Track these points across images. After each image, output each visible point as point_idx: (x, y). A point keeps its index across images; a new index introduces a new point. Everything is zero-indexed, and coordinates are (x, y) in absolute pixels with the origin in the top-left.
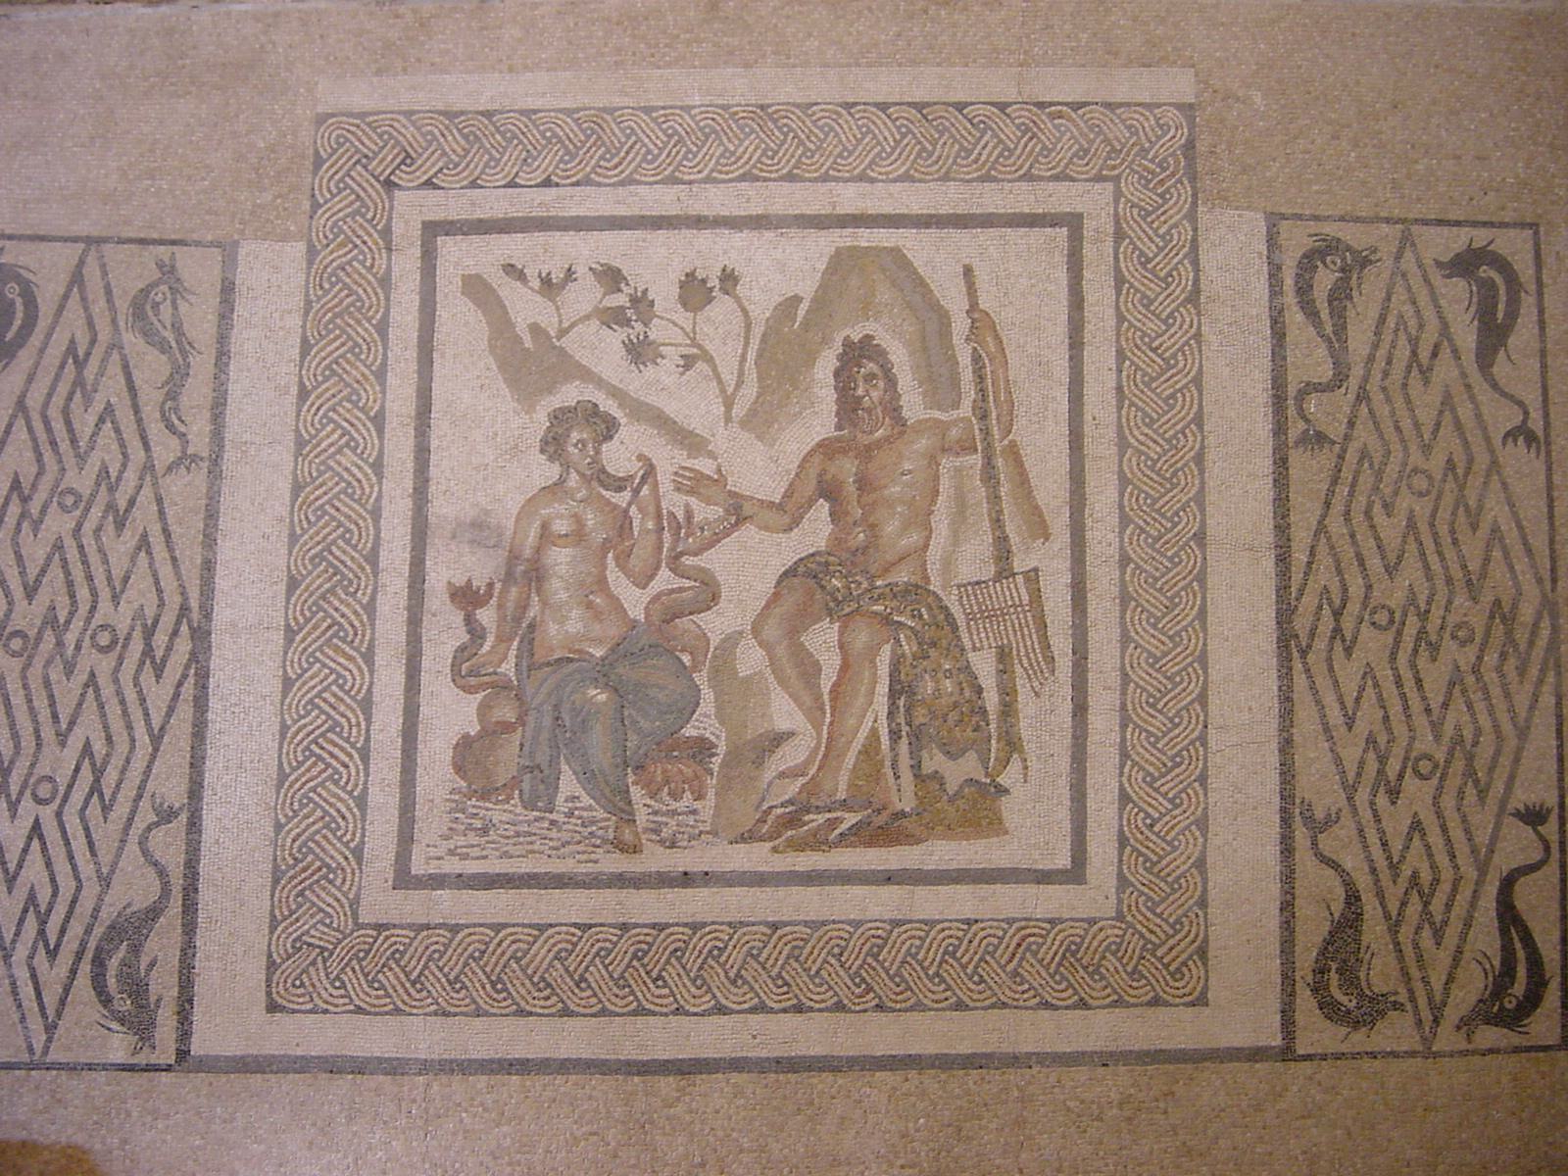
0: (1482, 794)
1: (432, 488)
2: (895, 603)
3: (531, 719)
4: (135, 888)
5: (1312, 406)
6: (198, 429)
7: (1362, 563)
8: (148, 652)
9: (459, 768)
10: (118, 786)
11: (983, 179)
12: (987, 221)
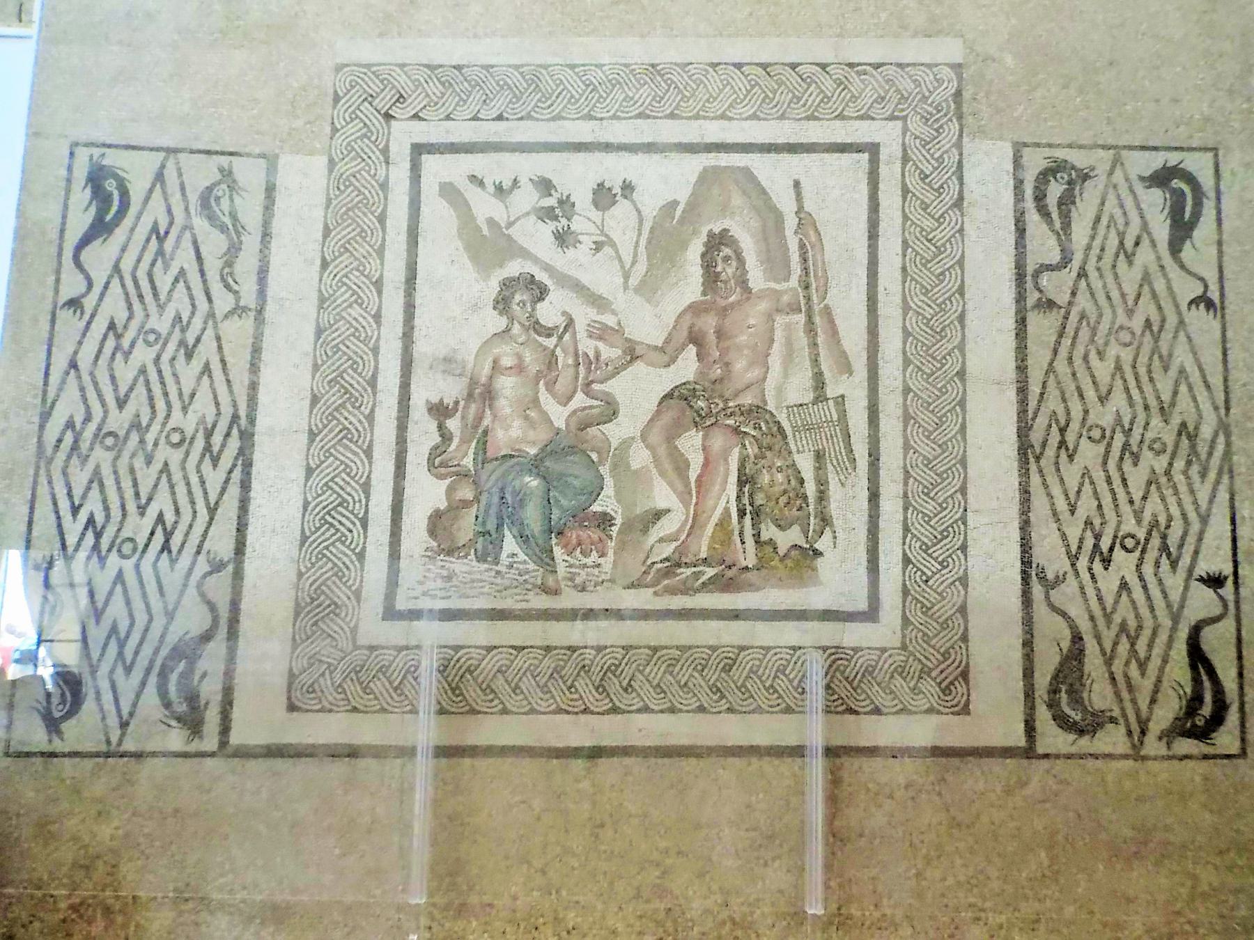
0: (1174, 564)
1: (416, 333)
2: (742, 418)
3: (484, 499)
4: (191, 620)
5: (1044, 280)
7: (1081, 396)
8: (208, 448)
9: (432, 532)
11: (808, 118)
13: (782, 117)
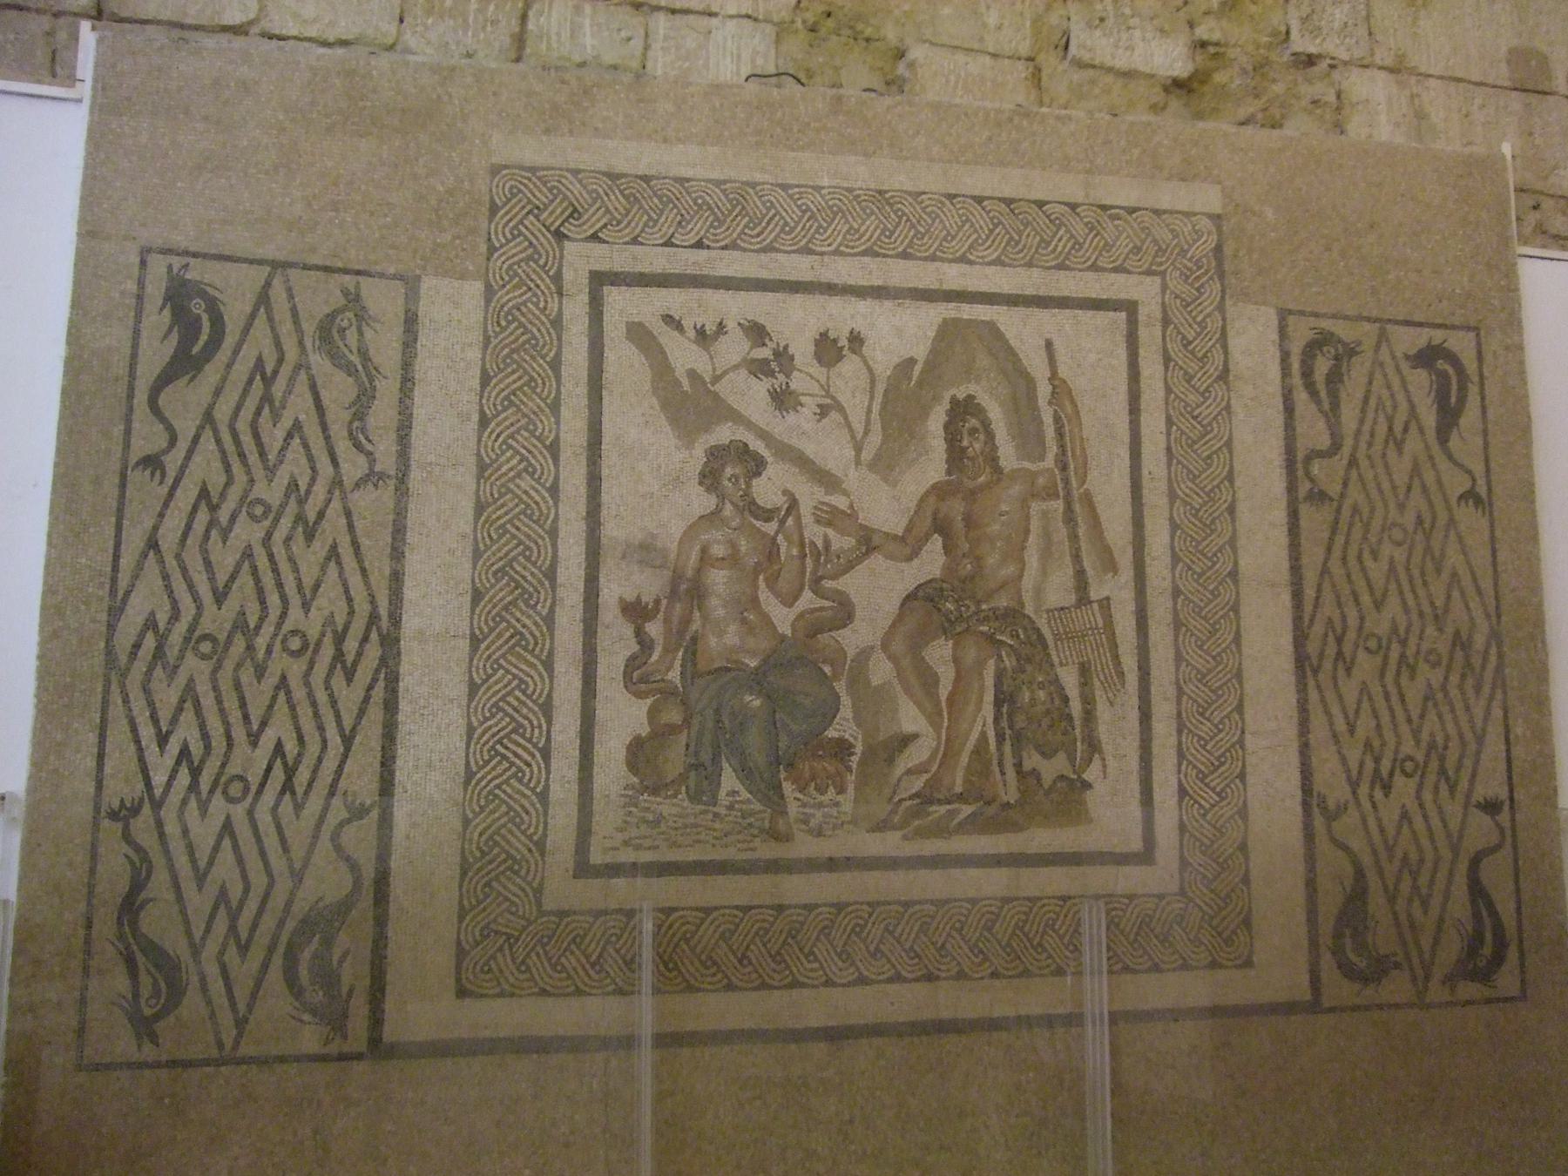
0: (1452, 789)
1: (604, 512)
2: (997, 624)
3: (695, 722)
4: (327, 882)
6: (385, 450)
8: (339, 655)
9: (632, 765)
10: (310, 785)
12: (1063, 303)
13: (1030, 265)
